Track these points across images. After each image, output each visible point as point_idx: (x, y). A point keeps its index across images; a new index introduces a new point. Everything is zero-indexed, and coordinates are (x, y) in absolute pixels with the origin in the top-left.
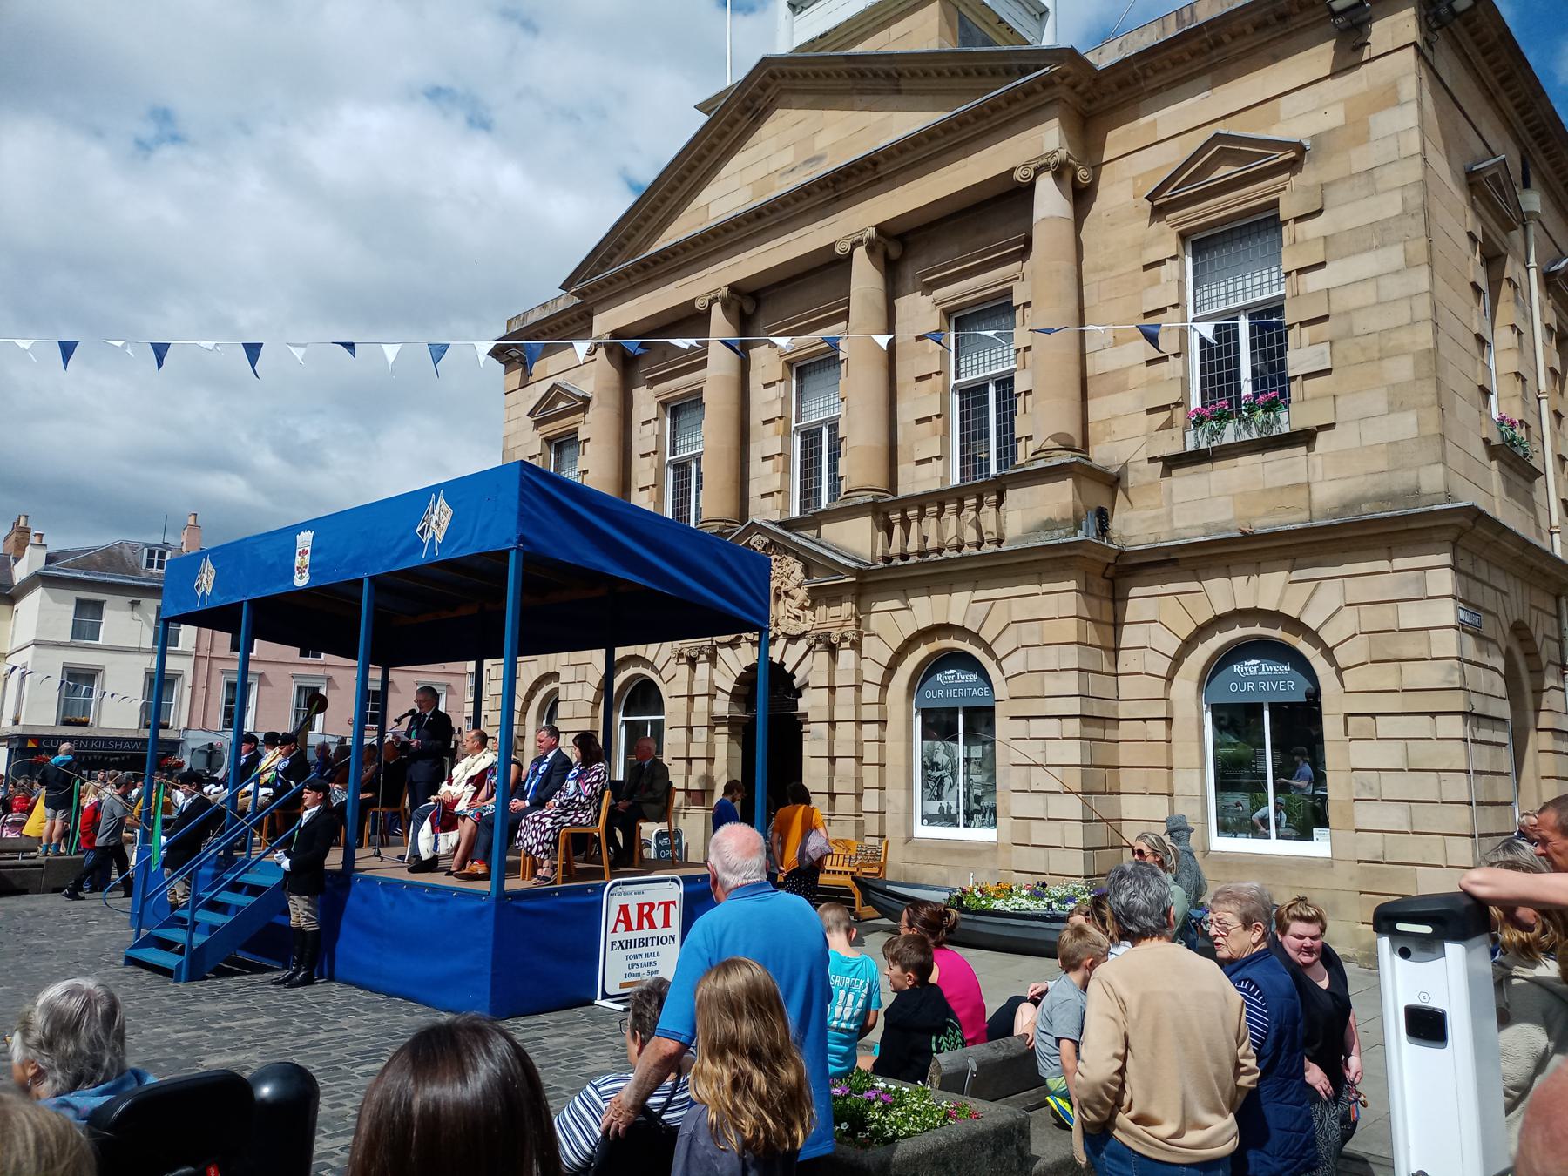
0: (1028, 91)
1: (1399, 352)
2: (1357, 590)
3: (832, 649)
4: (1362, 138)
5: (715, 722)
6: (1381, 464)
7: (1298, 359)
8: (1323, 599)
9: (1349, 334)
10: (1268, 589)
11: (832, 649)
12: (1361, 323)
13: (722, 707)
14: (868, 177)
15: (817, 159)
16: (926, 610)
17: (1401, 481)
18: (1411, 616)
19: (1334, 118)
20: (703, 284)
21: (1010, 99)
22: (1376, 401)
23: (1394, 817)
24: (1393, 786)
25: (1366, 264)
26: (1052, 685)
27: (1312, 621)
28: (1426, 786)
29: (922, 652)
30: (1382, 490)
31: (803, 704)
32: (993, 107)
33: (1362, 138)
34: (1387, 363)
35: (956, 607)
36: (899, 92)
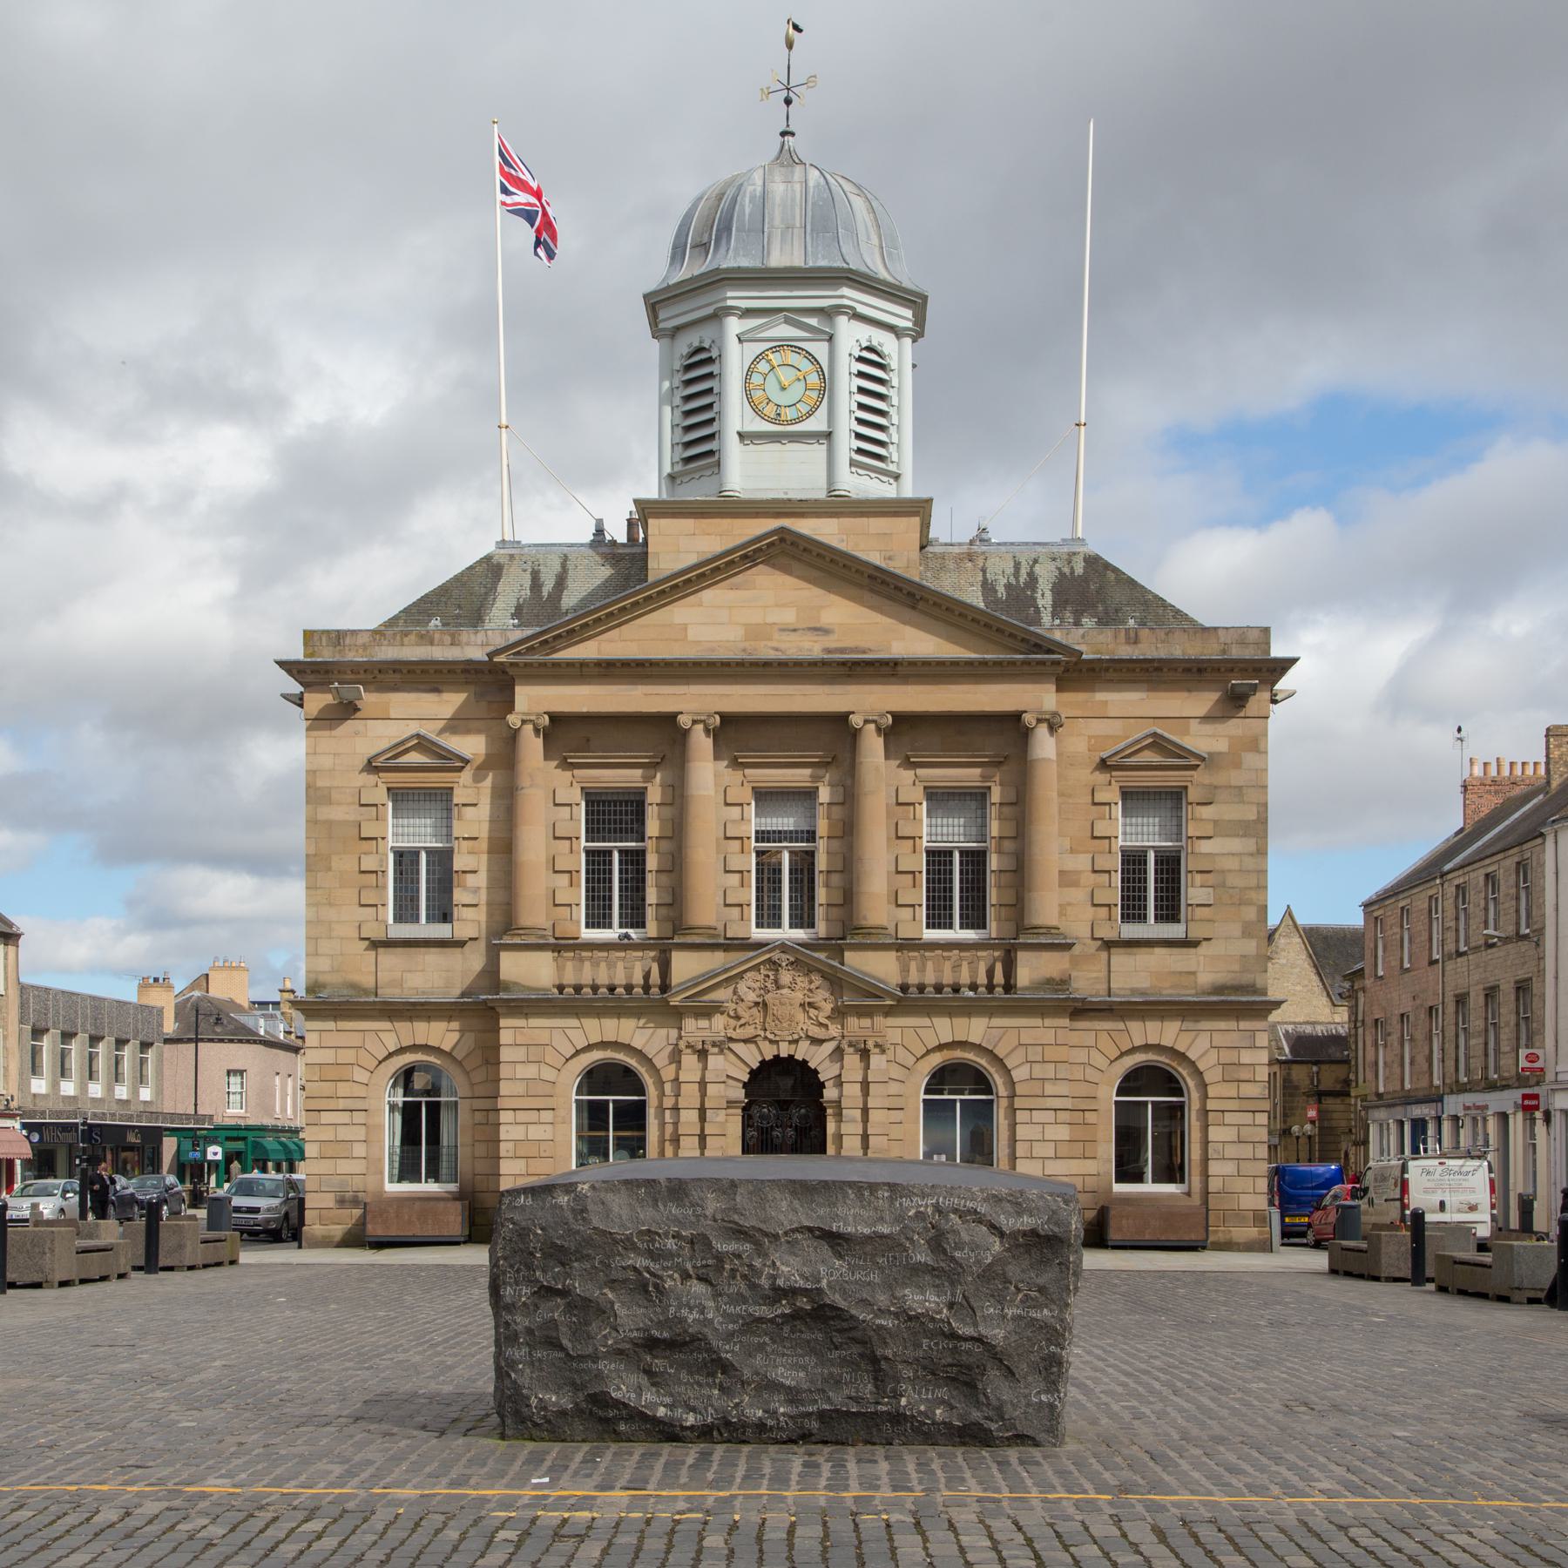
0: (1042, 663)
1: (1249, 903)
2: (1219, 1039)
3: (865, 1054)
4: (1237, 765)
5: (731, 1104)
6: (1236, 967)
7: (1194, 892)
8: (1201, 1044)
9: (1223, 885)
10: (1168, 1032)
11: (865, 1054)
12: (1233, 880)
13: (739, 1094)
14: (885, 670)
15: (824, 631)
16: (944, 1028)
17: (1246, 979)
18: (1246, 1057)
19: (1221, 746)
20: (692, 702)
21: (1026, 663)
22: (1235, 929)
23: (1230, 1168)
24: (1231, 1151)
25: (1235, 844)
26: (1050, 1089)
27: (1192, 1055)
28: (1247, 1151)
29: (936, 1060)
30: (1235, 983)
31: (830, 1093)
32: (1012, 663)
33: (1237, 765)
34: (1243, 908)
35: (976, 1029)
36: (914, 608)
